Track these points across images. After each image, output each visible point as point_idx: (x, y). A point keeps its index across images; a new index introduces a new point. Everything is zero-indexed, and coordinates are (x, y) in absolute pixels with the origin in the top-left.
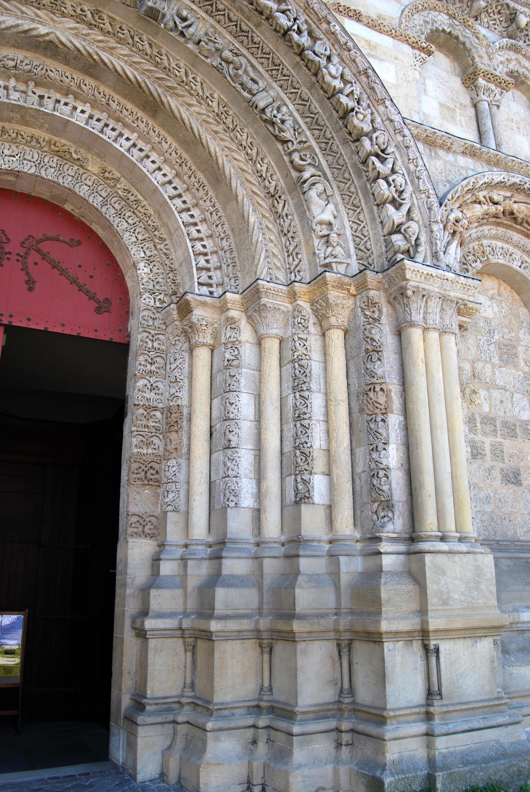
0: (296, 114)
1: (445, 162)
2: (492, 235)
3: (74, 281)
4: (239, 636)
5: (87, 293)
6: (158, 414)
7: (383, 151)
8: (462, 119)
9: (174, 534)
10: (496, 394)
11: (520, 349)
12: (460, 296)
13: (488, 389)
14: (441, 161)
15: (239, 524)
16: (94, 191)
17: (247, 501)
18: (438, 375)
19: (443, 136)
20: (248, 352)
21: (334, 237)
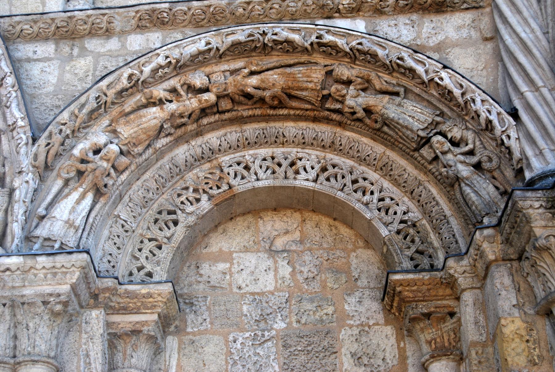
1: (98, 56)
2: (234, 144)
11: (344, 334)
12: (48, 289)
14: (89, 59)
19: (88, 16)
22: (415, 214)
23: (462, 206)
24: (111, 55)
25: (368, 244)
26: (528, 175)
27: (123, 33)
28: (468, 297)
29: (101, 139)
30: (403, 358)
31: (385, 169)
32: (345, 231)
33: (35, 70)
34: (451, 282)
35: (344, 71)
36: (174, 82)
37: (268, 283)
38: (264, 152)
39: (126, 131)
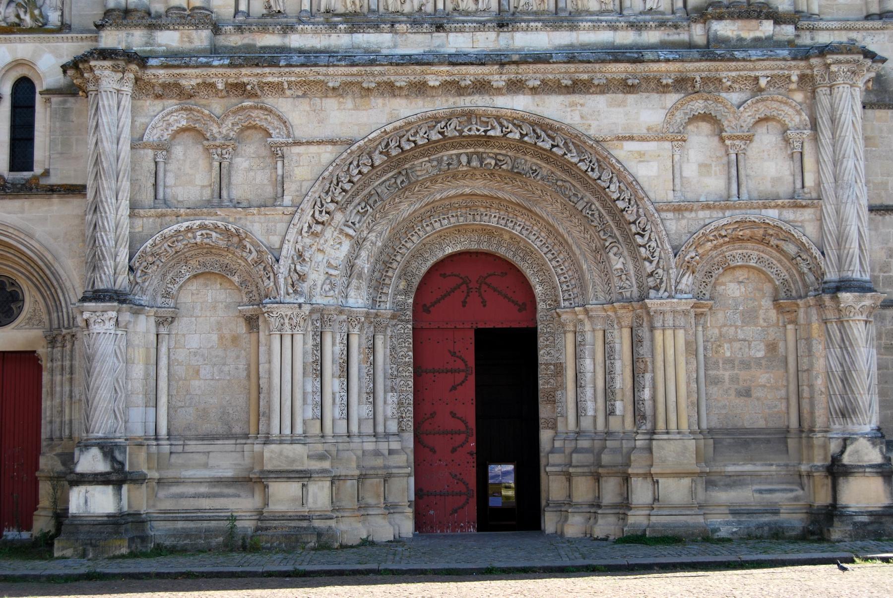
0: (600, 208)
3: (505, 297)
4: (583, 474)
5: (513, 302)
6: (552, 367)
7: (644, 230)
8: (717, 169)
9: (561, 427)
10: (737, 345)
11: (761, 312)
12: (684, 308)
13: (730, 343)
15: (586, 424)
16: (508, 249)
17: (590, 413)
18: (670, 352)
20: (589, 337)
21: (623, 276)
22: (787, 277)
23: (804, 281)
24: (692, 219)
25: (769, 281)
26: (825, 279)
27: (696, 211)
28: (802, 310)
29: (693, 254)
30: (778, 320)
31: (780, 261)
32: (762, 276)
33: (668, 223)
34: (798, 305)
35: (770, 232)
36: (715, 233)
37: (737, 294)
38: (740, 251)
39: (700, 251)
